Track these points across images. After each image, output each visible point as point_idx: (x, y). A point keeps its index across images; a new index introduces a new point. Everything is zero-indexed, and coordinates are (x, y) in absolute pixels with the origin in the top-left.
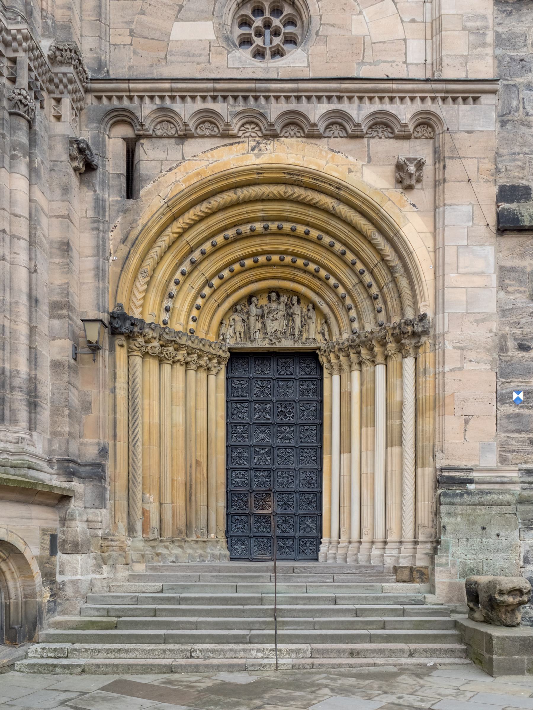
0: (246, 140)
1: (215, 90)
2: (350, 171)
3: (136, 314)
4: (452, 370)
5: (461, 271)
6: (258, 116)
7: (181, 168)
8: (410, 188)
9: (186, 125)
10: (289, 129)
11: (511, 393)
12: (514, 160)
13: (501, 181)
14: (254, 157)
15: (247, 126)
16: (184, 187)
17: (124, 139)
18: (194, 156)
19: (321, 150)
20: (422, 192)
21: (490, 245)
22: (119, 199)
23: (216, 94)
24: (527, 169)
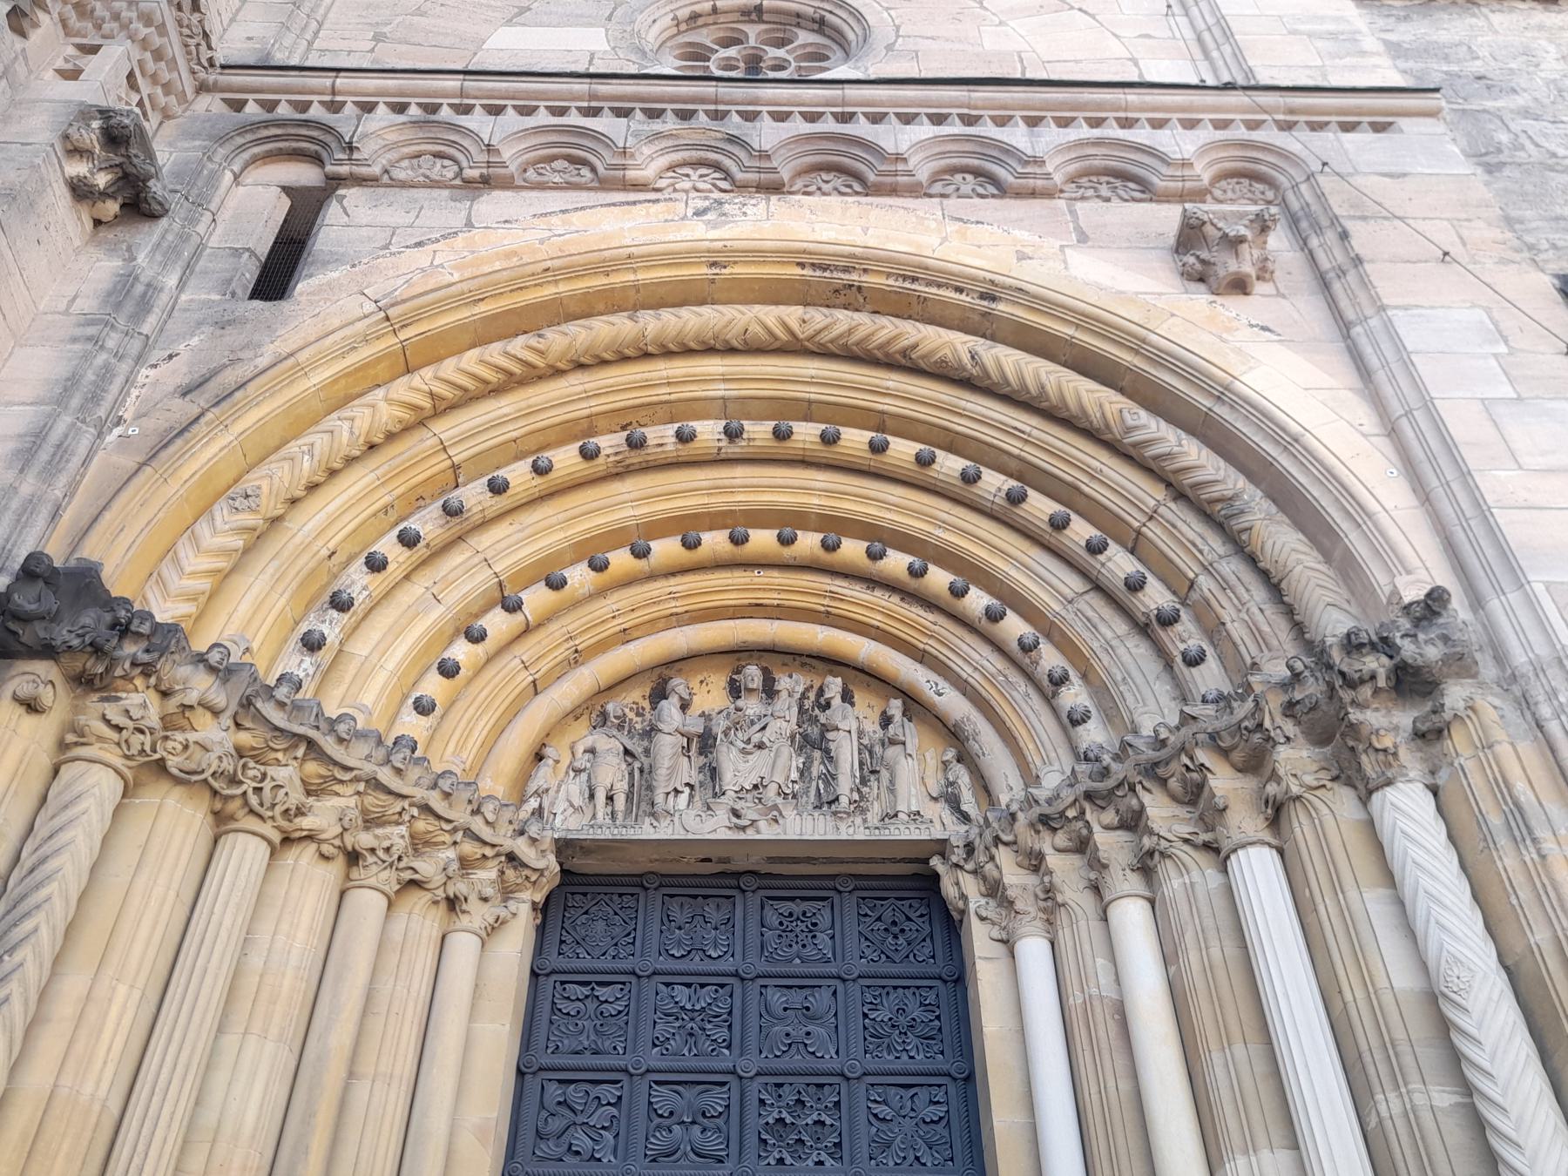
8: (1240, 286)
14: (702, 226)
18: (506, 222)
22: (217, 297)
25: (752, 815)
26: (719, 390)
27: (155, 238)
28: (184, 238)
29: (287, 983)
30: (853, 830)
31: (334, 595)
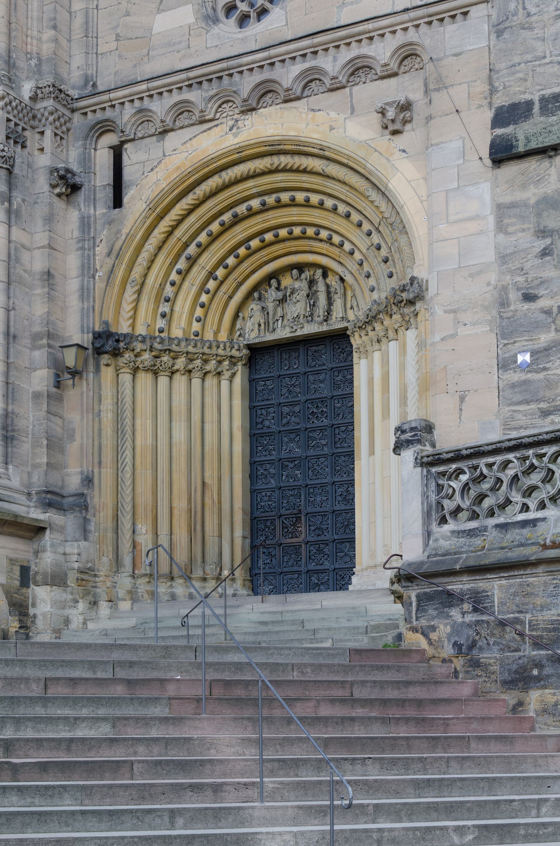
0: (224, 120)
1: (189, 79)
2: (332, 128)
3: (124, 328)
4: (443, 339)
5: (452, 218)
6: (232, 94)
7: (162, 165)
8: (395, 132)
9: (162, 121)
10: (267, 98)
11: (515, 356)
12: (514, 73)
13: (499, 101)
15: (225, 106)
16: (164, 186)
17: (110, 147)
19: (301, 113)
20: (413, 133)
21: (485, 181)
22: (105, 211)
23: (190, 82)
24: (530, 79)
25: (295, 327)
26: (254, 191)
27: (83, 196)
28: (89, 191)
29: (183, 407)
30: (325, 328)
31: (165, 298)
